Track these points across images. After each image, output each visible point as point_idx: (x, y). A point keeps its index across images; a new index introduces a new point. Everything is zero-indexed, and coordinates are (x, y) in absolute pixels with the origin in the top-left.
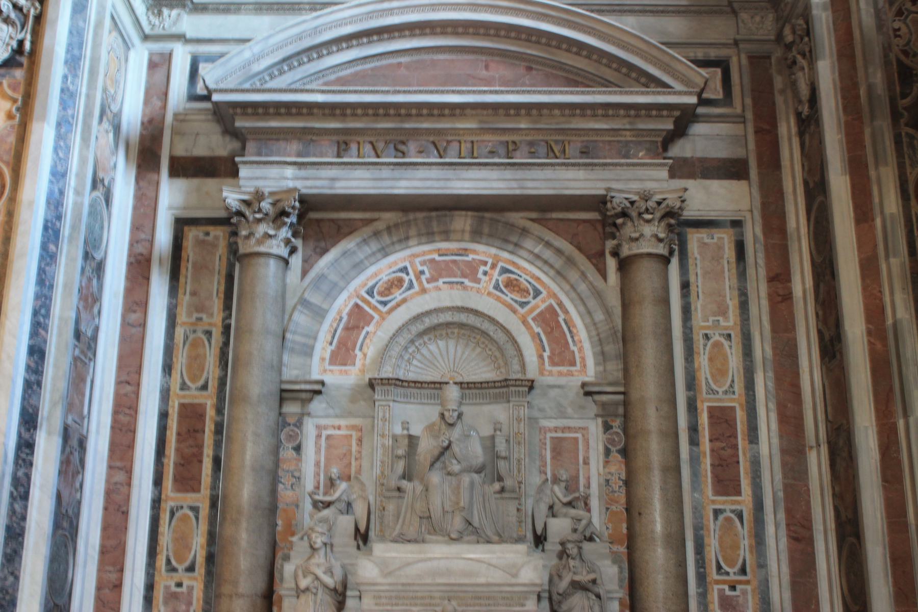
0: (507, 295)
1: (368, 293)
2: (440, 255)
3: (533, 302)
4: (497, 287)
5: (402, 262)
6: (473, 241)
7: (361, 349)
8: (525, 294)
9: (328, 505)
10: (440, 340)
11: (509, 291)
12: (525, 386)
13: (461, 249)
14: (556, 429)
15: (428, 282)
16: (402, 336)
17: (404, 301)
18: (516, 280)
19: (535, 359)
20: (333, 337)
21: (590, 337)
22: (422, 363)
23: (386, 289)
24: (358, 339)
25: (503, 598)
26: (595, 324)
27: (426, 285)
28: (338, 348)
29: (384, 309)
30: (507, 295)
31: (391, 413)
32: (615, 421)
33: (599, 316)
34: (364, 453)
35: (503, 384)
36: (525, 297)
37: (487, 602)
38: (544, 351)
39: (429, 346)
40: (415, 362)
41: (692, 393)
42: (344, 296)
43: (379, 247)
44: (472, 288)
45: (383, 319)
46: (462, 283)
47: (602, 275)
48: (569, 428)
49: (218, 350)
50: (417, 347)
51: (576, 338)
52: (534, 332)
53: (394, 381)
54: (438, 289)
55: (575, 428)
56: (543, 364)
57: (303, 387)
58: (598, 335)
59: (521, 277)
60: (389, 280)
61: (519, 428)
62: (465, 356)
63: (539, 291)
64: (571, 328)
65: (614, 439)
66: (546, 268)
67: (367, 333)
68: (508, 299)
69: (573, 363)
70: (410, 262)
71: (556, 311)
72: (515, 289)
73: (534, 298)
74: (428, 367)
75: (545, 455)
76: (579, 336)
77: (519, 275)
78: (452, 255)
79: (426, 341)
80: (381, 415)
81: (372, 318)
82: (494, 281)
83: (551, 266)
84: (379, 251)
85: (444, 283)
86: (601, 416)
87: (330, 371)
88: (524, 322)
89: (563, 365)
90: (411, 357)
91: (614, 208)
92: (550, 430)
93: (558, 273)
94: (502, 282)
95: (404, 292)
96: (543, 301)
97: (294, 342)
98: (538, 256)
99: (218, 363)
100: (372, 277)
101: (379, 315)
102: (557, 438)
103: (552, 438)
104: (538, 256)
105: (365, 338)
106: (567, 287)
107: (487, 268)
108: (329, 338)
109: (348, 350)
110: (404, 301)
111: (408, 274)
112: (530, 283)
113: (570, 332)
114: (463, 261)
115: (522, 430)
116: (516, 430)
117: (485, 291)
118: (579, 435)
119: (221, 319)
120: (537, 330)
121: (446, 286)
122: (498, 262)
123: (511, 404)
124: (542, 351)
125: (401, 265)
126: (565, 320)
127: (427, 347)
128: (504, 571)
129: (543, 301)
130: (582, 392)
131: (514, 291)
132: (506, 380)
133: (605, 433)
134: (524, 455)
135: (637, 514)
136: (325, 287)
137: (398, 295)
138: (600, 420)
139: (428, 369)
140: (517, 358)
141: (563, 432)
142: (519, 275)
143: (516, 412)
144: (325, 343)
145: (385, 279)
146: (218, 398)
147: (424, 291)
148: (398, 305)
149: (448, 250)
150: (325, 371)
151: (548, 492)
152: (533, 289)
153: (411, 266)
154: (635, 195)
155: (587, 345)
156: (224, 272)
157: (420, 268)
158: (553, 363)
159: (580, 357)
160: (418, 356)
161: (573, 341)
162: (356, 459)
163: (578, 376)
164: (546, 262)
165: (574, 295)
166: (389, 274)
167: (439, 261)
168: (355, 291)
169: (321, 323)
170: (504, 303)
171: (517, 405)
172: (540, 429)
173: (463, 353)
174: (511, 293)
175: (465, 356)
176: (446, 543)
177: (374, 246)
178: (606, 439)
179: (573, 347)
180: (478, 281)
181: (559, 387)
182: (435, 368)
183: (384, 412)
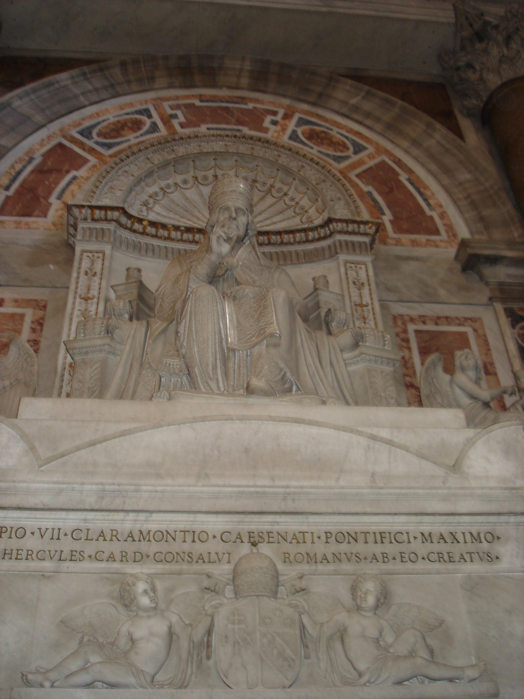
1: (81, 133)
3: (355, 158)
4: (294, 137)
5: (142, 104)
6: (253, 89)
7: (59, 197)
8: (341, 148)
11: (315, 144)
12: (366, 234)
14: (423, 319)
16: (136, 165)
21: (455, 202)
23: (113, 130)
24: (57, 183)
25: (427, 538)
28: (18, 192)
29: (107, 153)
30: (312, 148)
31: (107, 263)
35: (322, 232)
36: (341, 151)
37: (378, 549)
38: (383, 214)
40: (157, 208)
42: (43, 133)
48: (447, 318)
51: (432, 202)
52: (361, 190)
53: (116, 214)
55: (457, 318)
59: (332, 130)
60: (119, 122)
61: (361, 297)
64: (422, 190)
66: (368, 122)
67: (75, 178)
69: (437, 232)
70: (154, 105)
71: (393, 170)
73: (356, 153)
75: (411, 358)
78: (222, 102)
81: (86, 161)
82: (289, 132)
84: (105, 88)
89: (418, 232)
92: (412, 320)
94: (303, 134)
96: (371, 157)
100: (91, 117)
101: (97, 158)
102: (428, 332)
103: (417, 332)
106: (405, 144)
107: (279, 118)
108: (5, 181)
111: (150, 116)
112: (347, 138)
113: (421, 194)
115: (366, 299)
116: (356, 299)
118: (467, 329)
120: (366, 188)
125: (139, 107)
126: (409, 180)
128: (421, 456)
129: (371, 157)
130: (458, 267)
131: (322, 143)
132: (330, 221)
133: (513, 326)
140: (342, 202)
141: (437, 324)
142: (328, 128)
143: (352, 274)
145: (112, 120)
149: (216, 96)
152: (352, 144)
153: (156, 109)
155: (452, 211)
157: (170, 112)
159: (445, 225)
161: (429, 205)
163: (446, 247)
166: (120, 115)
168: (61, 130)
172: (395, 318)
174: (318, 146)
177: (98, 82)
178: (519, 335)
180: (266, 130)
181: (417, 259)
183: (93, 262)
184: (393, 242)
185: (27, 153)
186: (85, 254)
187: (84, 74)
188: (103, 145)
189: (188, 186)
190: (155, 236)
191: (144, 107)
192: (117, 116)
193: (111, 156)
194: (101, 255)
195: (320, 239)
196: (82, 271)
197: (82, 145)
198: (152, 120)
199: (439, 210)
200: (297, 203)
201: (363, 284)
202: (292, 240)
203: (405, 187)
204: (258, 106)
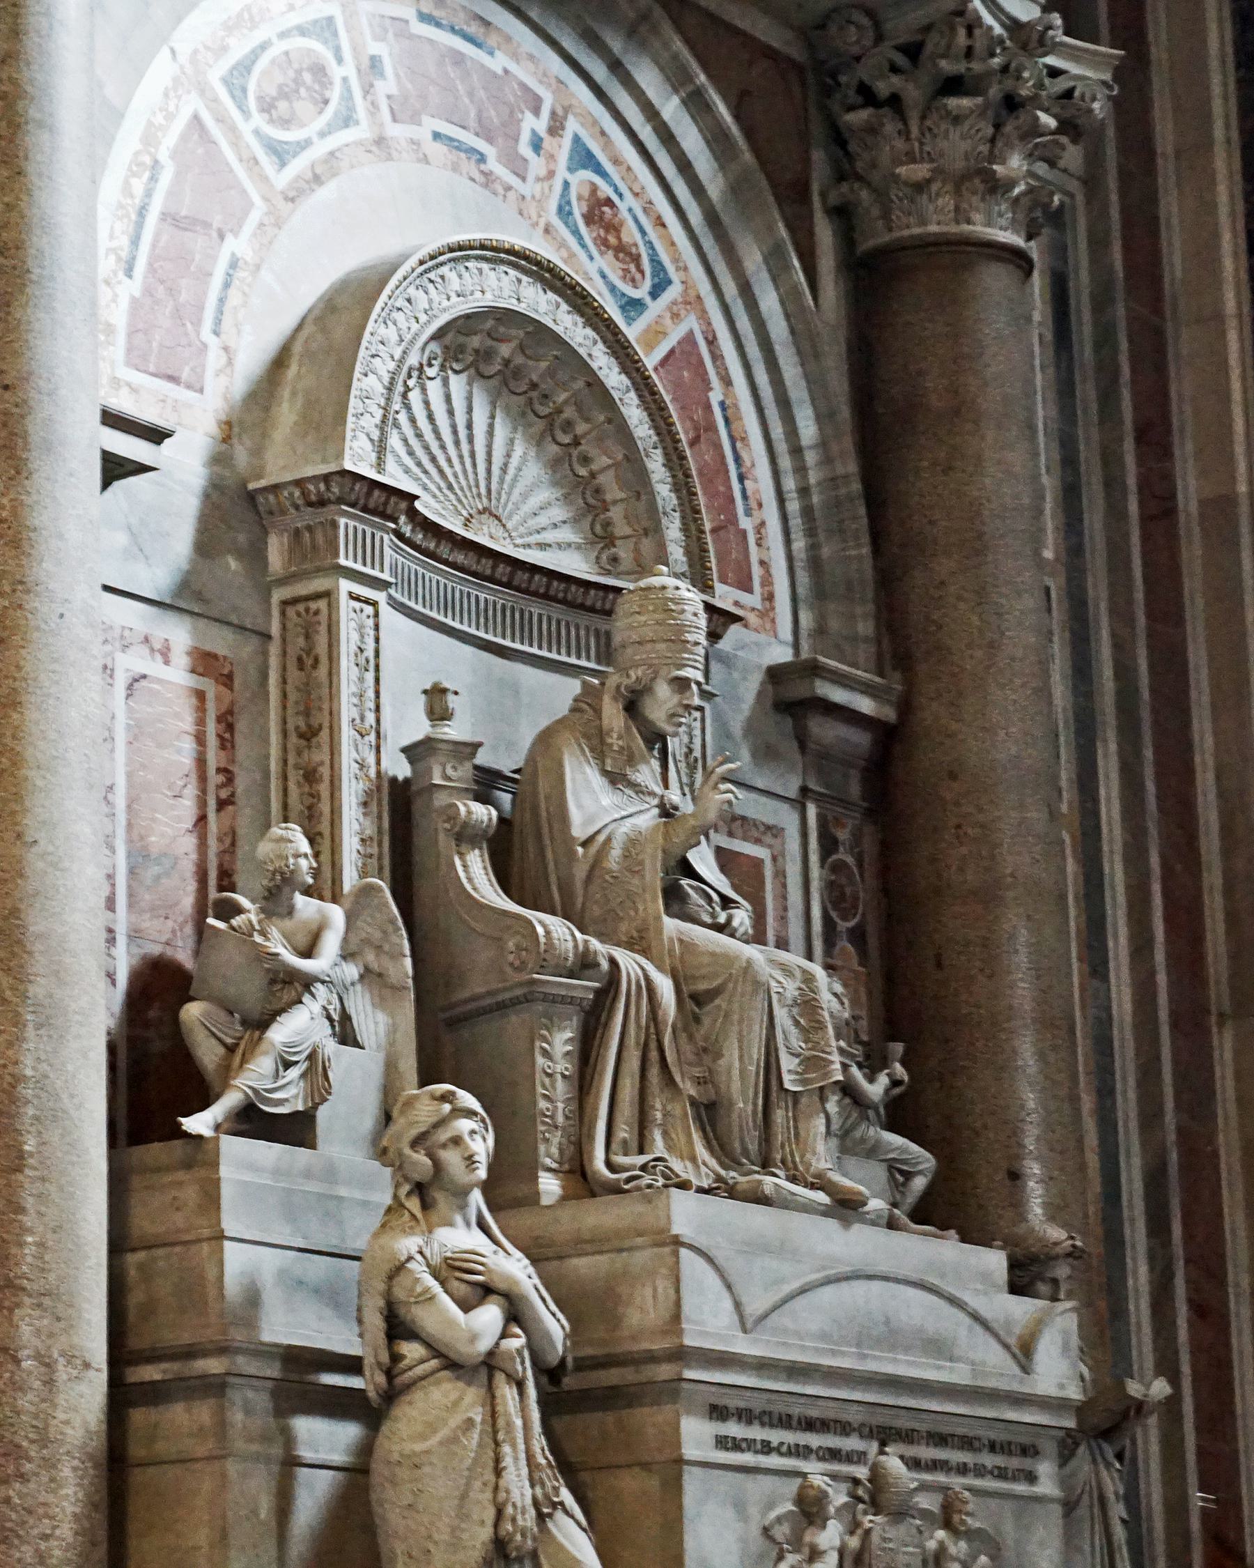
26: (796, 451)
34: (241, 784)
44: (509, 188)
58: (804, 491)
74: (426, 472)
76: (756, 481)
83: (697, 189)
85: (437, 136)
86: (819, 799)
91: (969, 53)
93: (712, 219)
113: (738, 459)
126: (722, 404)
135: (1000, 1176)
138: (812, 811)
154: (1003, 25)
162: (222, 804)
164: (684, 166)
176: (826, 1212)
200: (593, 475)
201: (696, 760)
202: (599, 605)
204: (513, 67)
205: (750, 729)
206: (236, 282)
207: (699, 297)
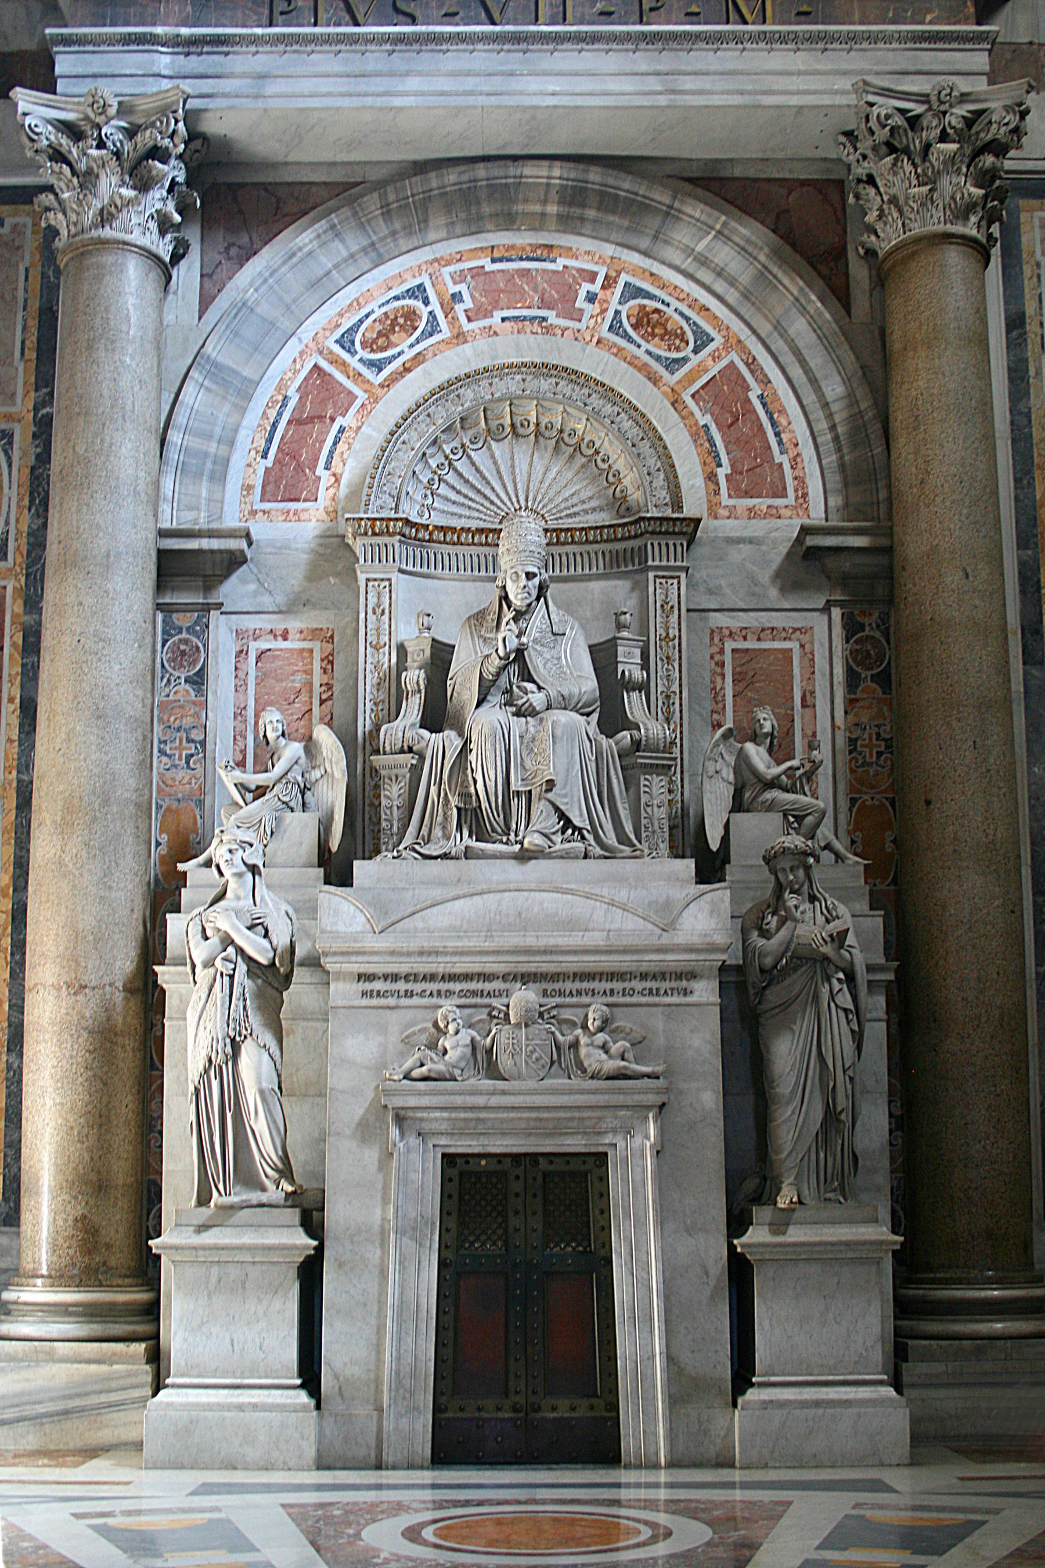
0: (639, 346)
2: (494, 261)
3: (695, 360)
8: (677, 342)
9: (260, 792)
10: (498, 441)
11: (642, 337)
13: (540, 246)
15: (469, 320)
17: (419, 359)
18: (657, 311)
19: (699, 481)
20: (270, 440)
22: (459, 492)
23: (380, 334)
26: (826, 405)
27: (467, 326)
28: (277, 461)
32: (870, 614)
33: (834, 388)
38: (720, 465)
39: (472, 453)
41: (1030, 552)
42: (292, 349)
43: (365, 242)
45: (376, 401)
46: (544, 319)
47: (839, 300)
49: (28, 471)
50: (446, 457)
52: (696, 423)
54: (491, 332)
56: (717, 492)
57: (205, 544)
58: (833, 428)
59: (668, 305)
60: (386, 313)
62: (551, 475)
63: (708, 335)
65: (868, 651)
66: (720, 287)
67: (342, 430)
68: (640, 353)
72: (657, 331)
73: (696, 351)
74: (471, 499)
77: (663, 302)
78: (521, 259)
79: (466, 441)
80: (372, 600)
81: (352, 397)
82: (610, 314)
83: (732, 282)
85: (503, 320)
86: (840, 604)
87: (264, 512)
88: (676, 403)
89: (759, 496)
90: (436, 478)
94: (628, 317)
95: (418, 341)
96: (715, 357)
97: (183, 449)
98: (703, 261)
99: (26, 502)
101: (366, 391)
104: (703, 261)
105: (335, 443)
109: (299, 468)
110: (419, 359)
111: (426, 302)
112: (687, 319)
113: (774, 424)
114: (545, 271)
117: (592, 336)
119: (31, 407)
120: (705, 419)
121: (507, 324)
122: (619, 273)
123: (651, 575)
124: (714, 465)
126: (761, 397)
127: (469, 457)
129: (715, 357)
131: (653, 335)
134: (680, 685)
136: (249, 332)
137: (405, 347)
138: (836, 613)
139: (470, 503)
142: (663, 302)
144: (253, 453)
145: (378, 313)
146: (27, 576)
147: (460, 337)
148: (406, 370)
149: (512, 247)
150: (253, 513)
151: (731, 760)
152: (694, 333)
155: (808, 452)
156: (35, 305)
157: (453, 289)
158: (737, 492)
159: (796, 478)
160: (451, 478)
161: (780, 443)
165: (779, 345)
166: (388, 302)
167: (493, 272)
169: (243, 411)
170: (633, 362)
171: (664, 577)
173: (547, 469)
174: (648, 342)
175: (551, 475)
177: (355, 241)
179: (778, 458)
181: (750, 541)
182: (487, 504)
184: (726, 513)
185: (279, 389)
186: (370, 584)
187: (333, 227)
188: (371, 364)
189: (480, 445)
190: (445, 542)
191: (418, 281)
192: (383, 304)
193: (381, 386)
194: (387, 583)
195: (630, 538)
196: (370, 611)
197: (343, 366)
198: (429, 308)
199: (792, 453)
203: (754, 411)
205: (778, 575)
206: (343, 439)
207: (739, 341)
